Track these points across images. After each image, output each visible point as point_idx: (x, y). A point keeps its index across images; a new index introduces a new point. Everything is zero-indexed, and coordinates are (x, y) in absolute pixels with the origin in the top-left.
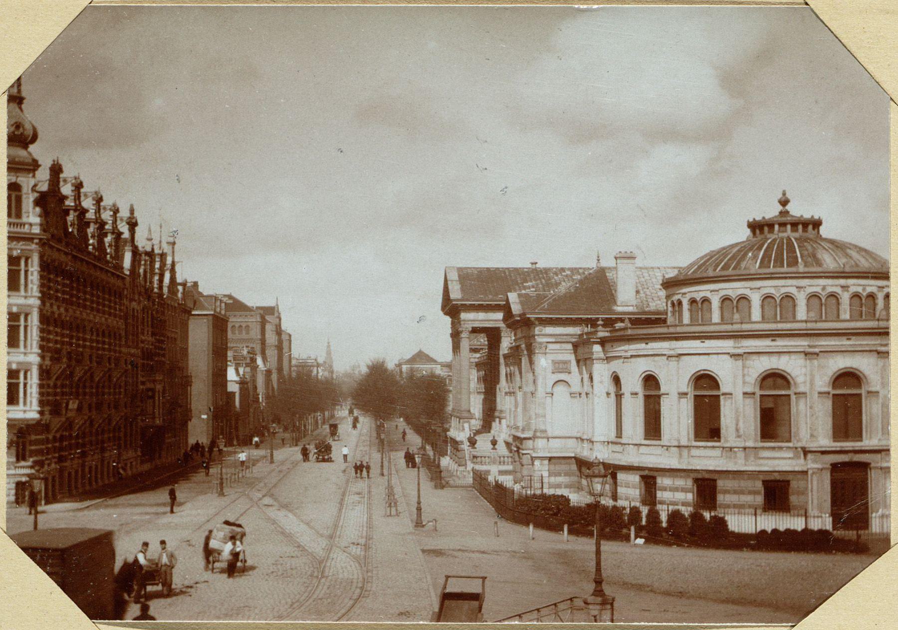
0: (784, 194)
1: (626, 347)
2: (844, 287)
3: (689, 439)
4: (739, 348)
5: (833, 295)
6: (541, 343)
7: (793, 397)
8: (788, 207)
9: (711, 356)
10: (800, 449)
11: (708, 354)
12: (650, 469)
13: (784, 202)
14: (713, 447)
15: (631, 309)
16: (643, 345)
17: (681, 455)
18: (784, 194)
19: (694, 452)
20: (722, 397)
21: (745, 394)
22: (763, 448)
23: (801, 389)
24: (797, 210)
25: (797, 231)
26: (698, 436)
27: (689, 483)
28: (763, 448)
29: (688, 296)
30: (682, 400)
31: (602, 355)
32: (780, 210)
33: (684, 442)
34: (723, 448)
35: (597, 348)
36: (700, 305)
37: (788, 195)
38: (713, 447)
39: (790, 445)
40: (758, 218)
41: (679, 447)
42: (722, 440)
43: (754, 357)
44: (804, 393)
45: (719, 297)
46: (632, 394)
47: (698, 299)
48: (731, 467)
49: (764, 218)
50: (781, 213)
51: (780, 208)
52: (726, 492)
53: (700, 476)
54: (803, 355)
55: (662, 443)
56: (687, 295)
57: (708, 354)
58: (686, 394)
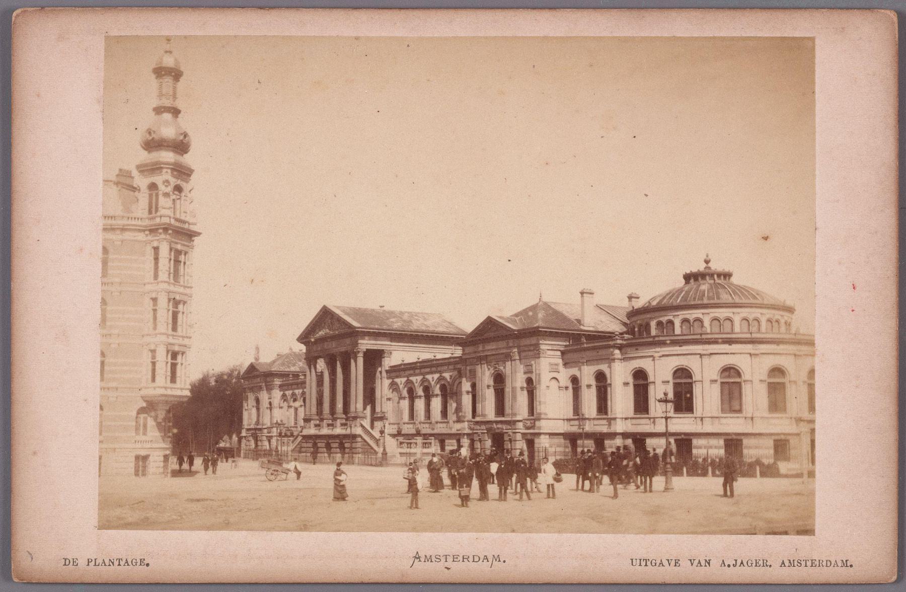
0: (707, 256)
1: (658, 349)
2: (782, 316)
3: (719, 413)
4: (756, 349)
5: (757, 320)
6: (543, 350)
7: (788, 385)
8: (710, 265)
9: (735, 355)
10: (793, 419)
11: (734, 354)
12: (685, 434)
13: (707, 262)
14: (738, 417)
15: (591, 329)
16: (677, 348)
17: (712, 424)
18: (707, 256)
19: (723, 421)
20: (743, 384)
21: (761, 381)
22: (771, 418)
23: (793, 379)
24: (715, 266)
25: (720, 279)
26: (723, 411)
27: (721, 442)
28: (771, 418)
29: (681, 317)
30: (713, 385)
31: (620, 356)
32: (705, 267)
33: (716, 415)
34: (746, 418)
35: (617, 352)
36: (665, 326)
37: (710, 257)
38: (738, 417)
39: (787, 415)
40: (688, 272)
41: (712, 417)
42: (744, 413)
43: (765, 356)
44: (795, 382)
45: (710, 317)
46: (663, 382)
47: (664, 322)
48: (749, 430)
49: (699, 270)
50: (705, 268)
51: (705, 265)
52: (750, 448)
53: (730, 437)
54: (793, 357)
55: (695, 415)
56: (679, 317)
57: (734, 354)
58: (716, 381)
